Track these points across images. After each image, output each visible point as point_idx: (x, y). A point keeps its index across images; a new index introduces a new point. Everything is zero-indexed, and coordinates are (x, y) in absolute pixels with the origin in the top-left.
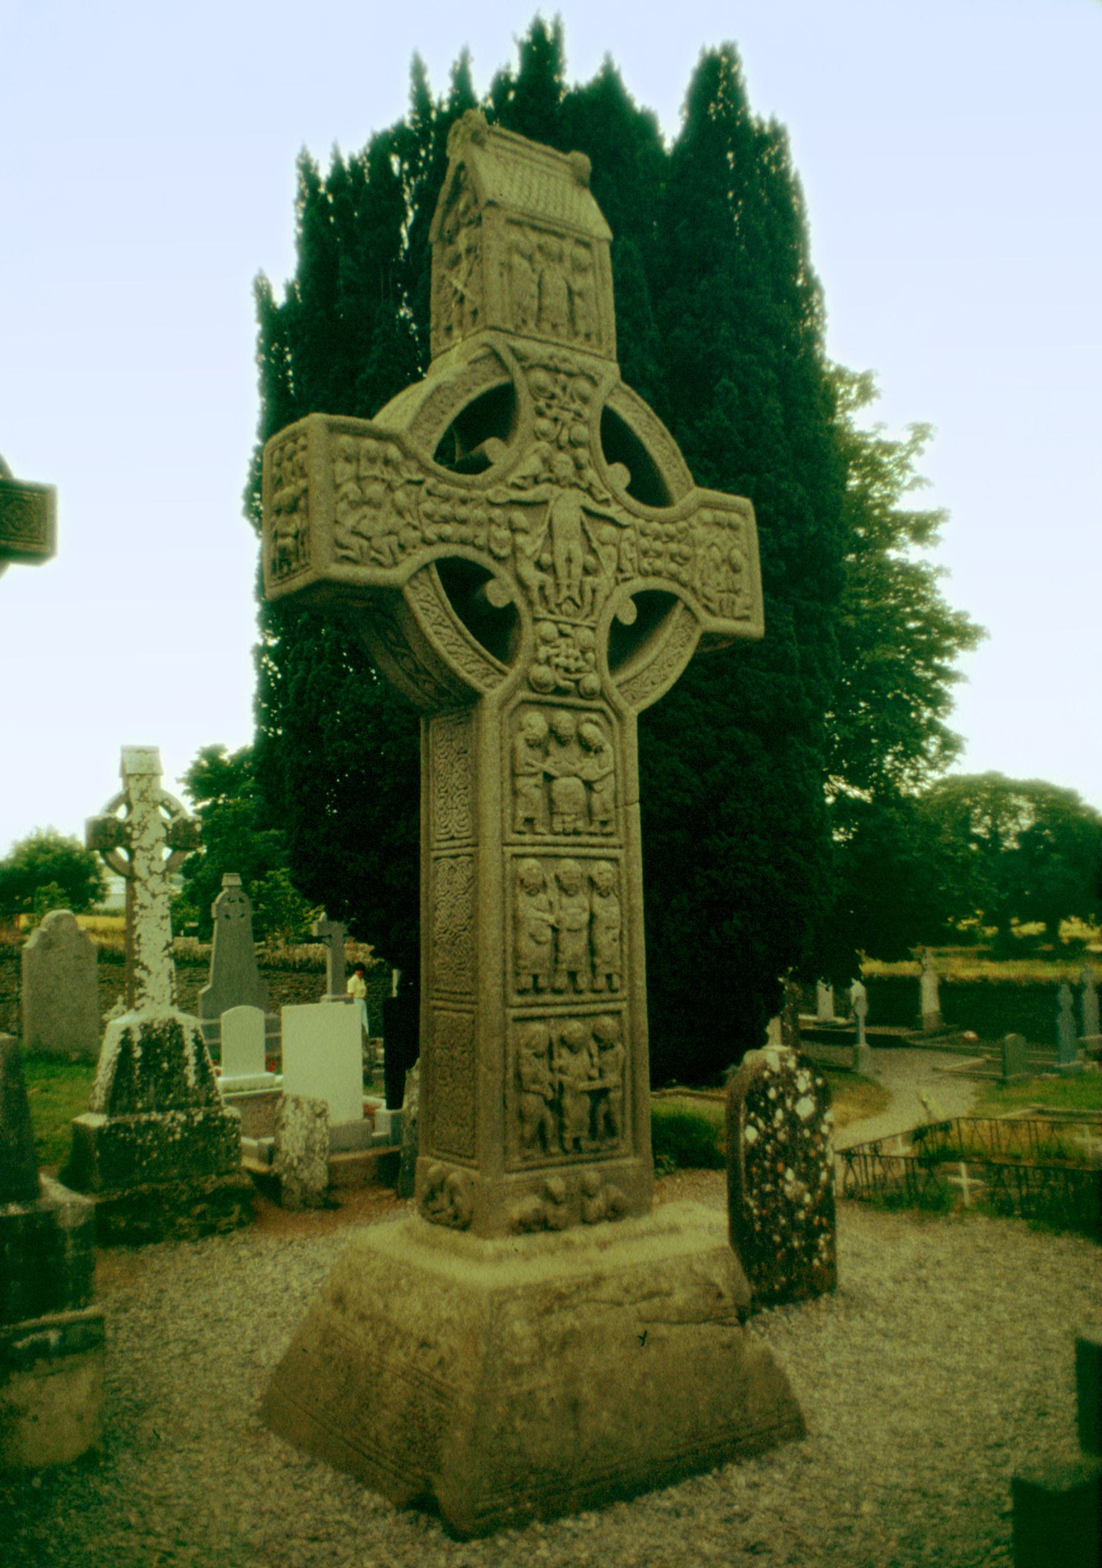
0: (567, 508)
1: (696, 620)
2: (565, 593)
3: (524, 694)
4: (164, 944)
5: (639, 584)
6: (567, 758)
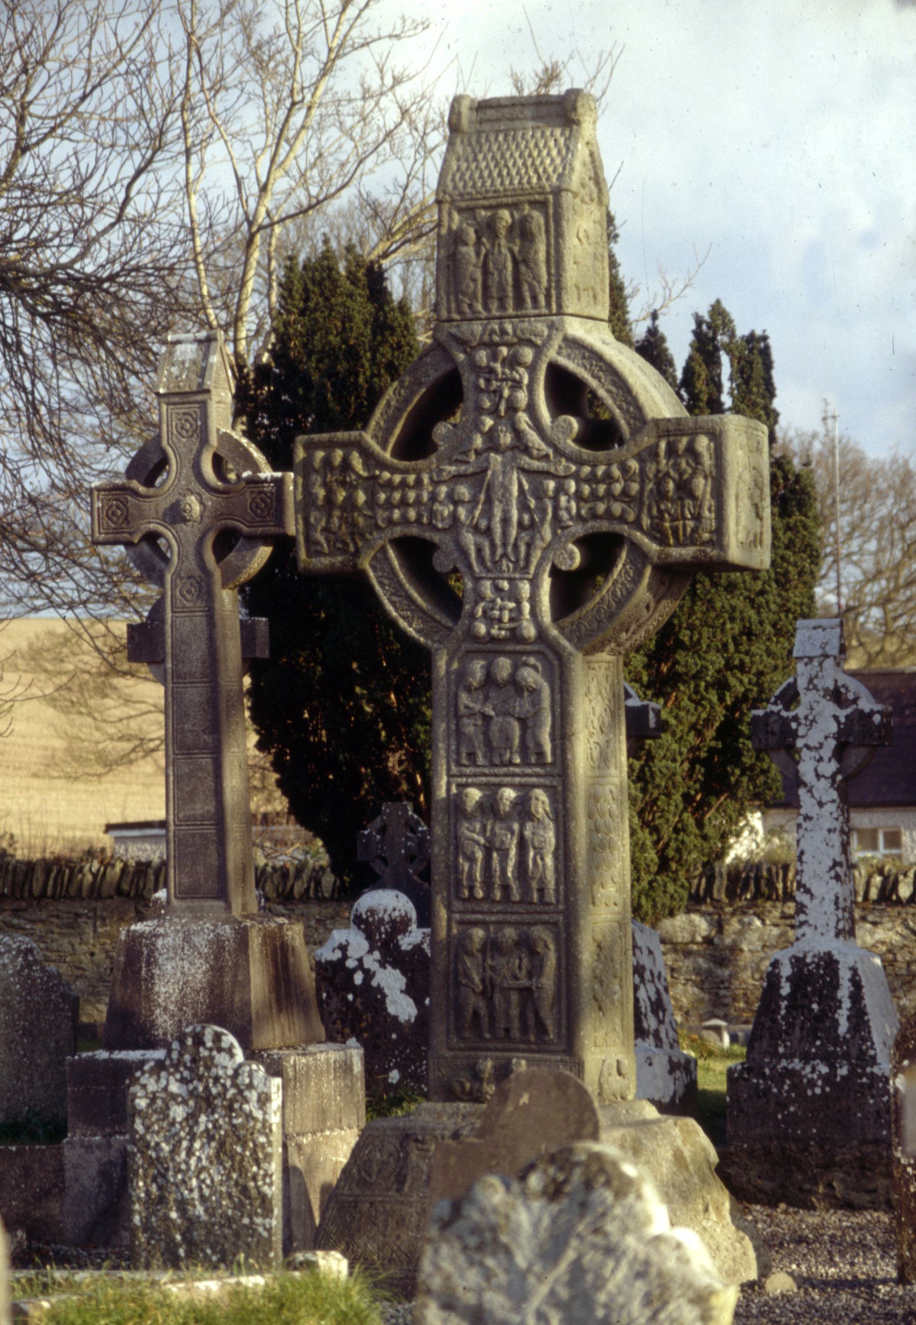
2: (499, 551)
4: (830, 863)
5: (579, 530)
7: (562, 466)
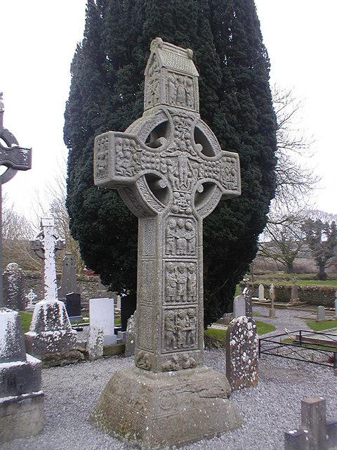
0: (184, 157)
1: (221, 190)
3: (170, 214)
5: (205, 180)
6: (182, 232)
7: (200, 160)
